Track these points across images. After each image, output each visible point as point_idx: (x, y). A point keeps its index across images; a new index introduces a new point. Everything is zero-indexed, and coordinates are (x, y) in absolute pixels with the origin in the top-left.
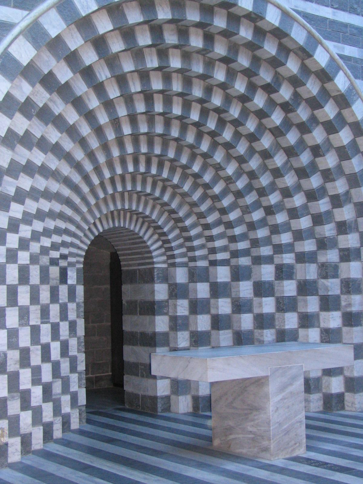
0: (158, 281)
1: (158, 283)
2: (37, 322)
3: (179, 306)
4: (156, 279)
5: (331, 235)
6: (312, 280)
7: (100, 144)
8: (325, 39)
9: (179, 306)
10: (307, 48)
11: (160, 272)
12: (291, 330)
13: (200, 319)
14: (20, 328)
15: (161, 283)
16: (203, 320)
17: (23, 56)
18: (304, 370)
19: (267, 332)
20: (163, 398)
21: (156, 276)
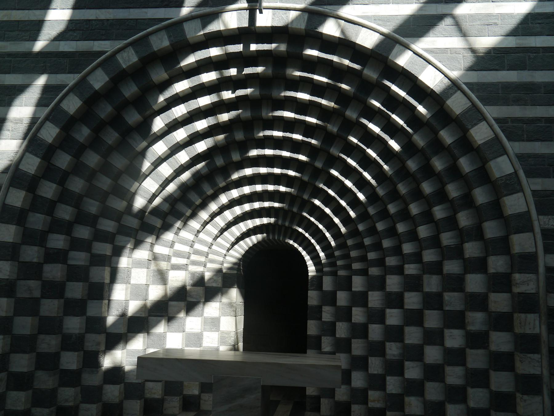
0: (312, 288)
1: (311, 290)
2: (141, 314)
3: (324, 312)
4: (309, 286)
5: (452, 244)
6: (433, 293)
7: (208, 169)
8: (403, 37)
9: (324, 312)
10: (379, 51)
11: (314, 280)
12: (413, 345)
13: (340, 326)
14: (85, 317)
15: (313, 290)
16: (343, 327)
17: (71, 107)
18: (262, 384)
19: (391, 344)
20: (312, 397)
21: (309, 284)
